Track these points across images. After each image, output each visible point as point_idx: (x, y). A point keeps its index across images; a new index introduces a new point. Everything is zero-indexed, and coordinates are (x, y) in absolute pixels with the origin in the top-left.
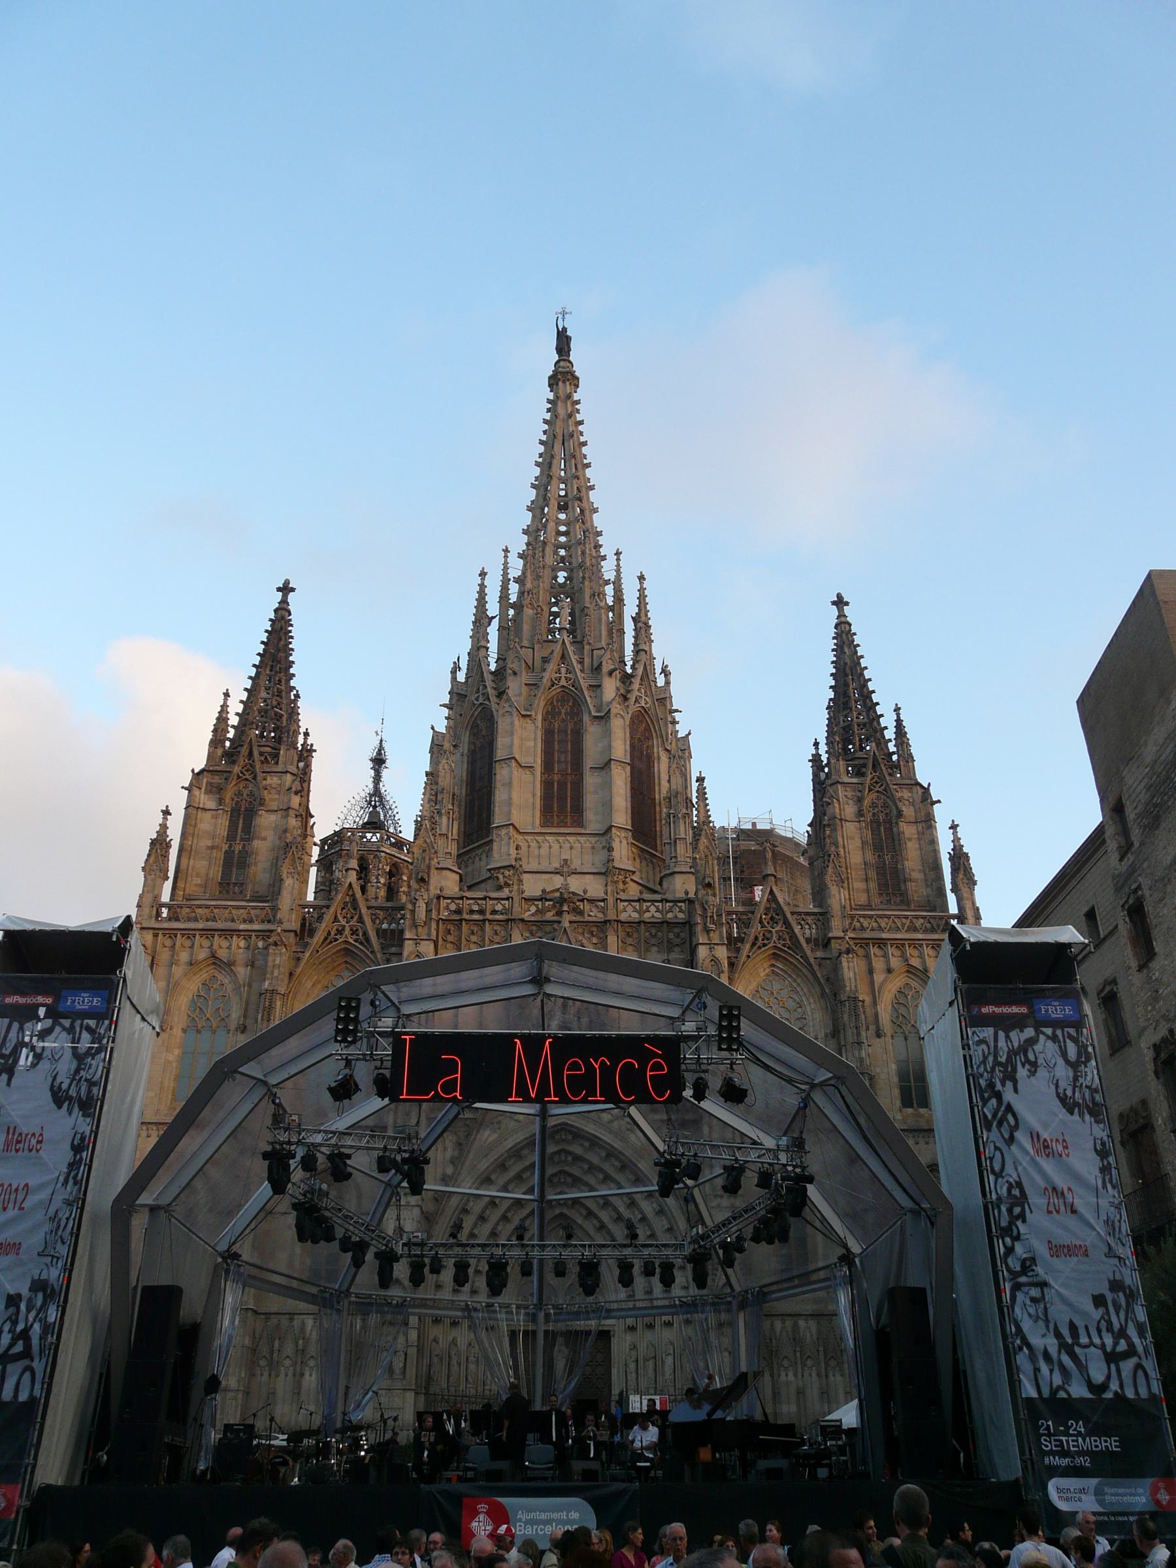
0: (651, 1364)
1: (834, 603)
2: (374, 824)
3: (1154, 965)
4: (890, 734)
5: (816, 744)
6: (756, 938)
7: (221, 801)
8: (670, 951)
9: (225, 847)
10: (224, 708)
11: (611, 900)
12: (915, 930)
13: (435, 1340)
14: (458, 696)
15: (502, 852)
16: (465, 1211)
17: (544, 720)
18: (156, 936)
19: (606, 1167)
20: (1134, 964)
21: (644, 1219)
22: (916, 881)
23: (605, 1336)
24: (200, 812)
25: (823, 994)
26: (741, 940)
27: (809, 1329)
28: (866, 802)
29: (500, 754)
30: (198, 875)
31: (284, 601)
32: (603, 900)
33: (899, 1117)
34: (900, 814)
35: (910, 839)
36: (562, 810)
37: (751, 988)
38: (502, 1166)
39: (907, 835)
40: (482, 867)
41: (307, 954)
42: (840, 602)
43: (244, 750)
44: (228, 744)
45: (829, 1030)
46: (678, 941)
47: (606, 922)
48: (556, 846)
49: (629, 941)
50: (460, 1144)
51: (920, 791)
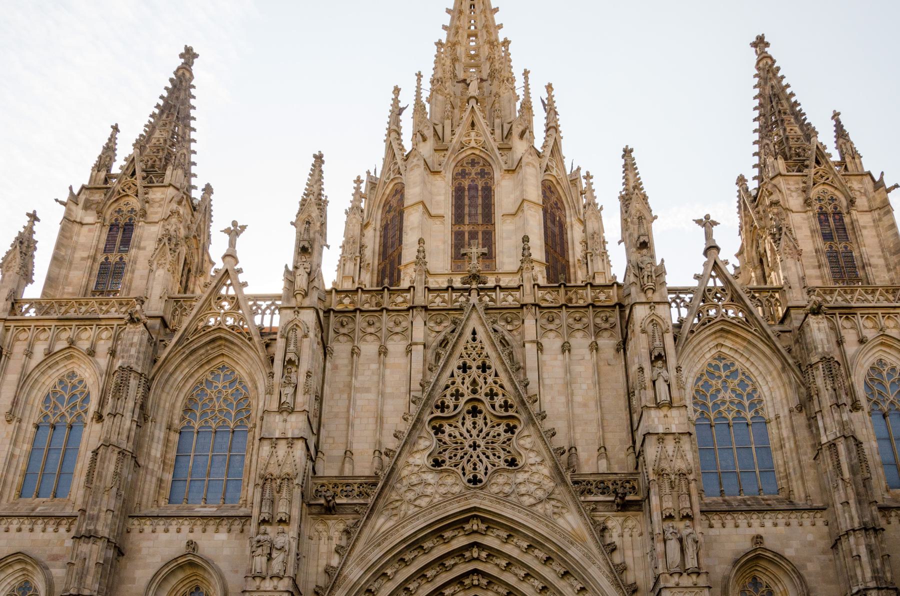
7: (99, 213)
9: (101, 258)
10: (112, 139)
11: (528, 286)
19: (528, 559)
22: (876, 266)
24: (76, 227)
28: (813, 193)
30: (69, 284)
32: (518, 288)
33: (886, 496)
34: (852, 202)
35: (865, 227)
37: (695, 370)
45: (793, 405)
47: (522, 306)
49: (551, 326)
50: (347, 532)
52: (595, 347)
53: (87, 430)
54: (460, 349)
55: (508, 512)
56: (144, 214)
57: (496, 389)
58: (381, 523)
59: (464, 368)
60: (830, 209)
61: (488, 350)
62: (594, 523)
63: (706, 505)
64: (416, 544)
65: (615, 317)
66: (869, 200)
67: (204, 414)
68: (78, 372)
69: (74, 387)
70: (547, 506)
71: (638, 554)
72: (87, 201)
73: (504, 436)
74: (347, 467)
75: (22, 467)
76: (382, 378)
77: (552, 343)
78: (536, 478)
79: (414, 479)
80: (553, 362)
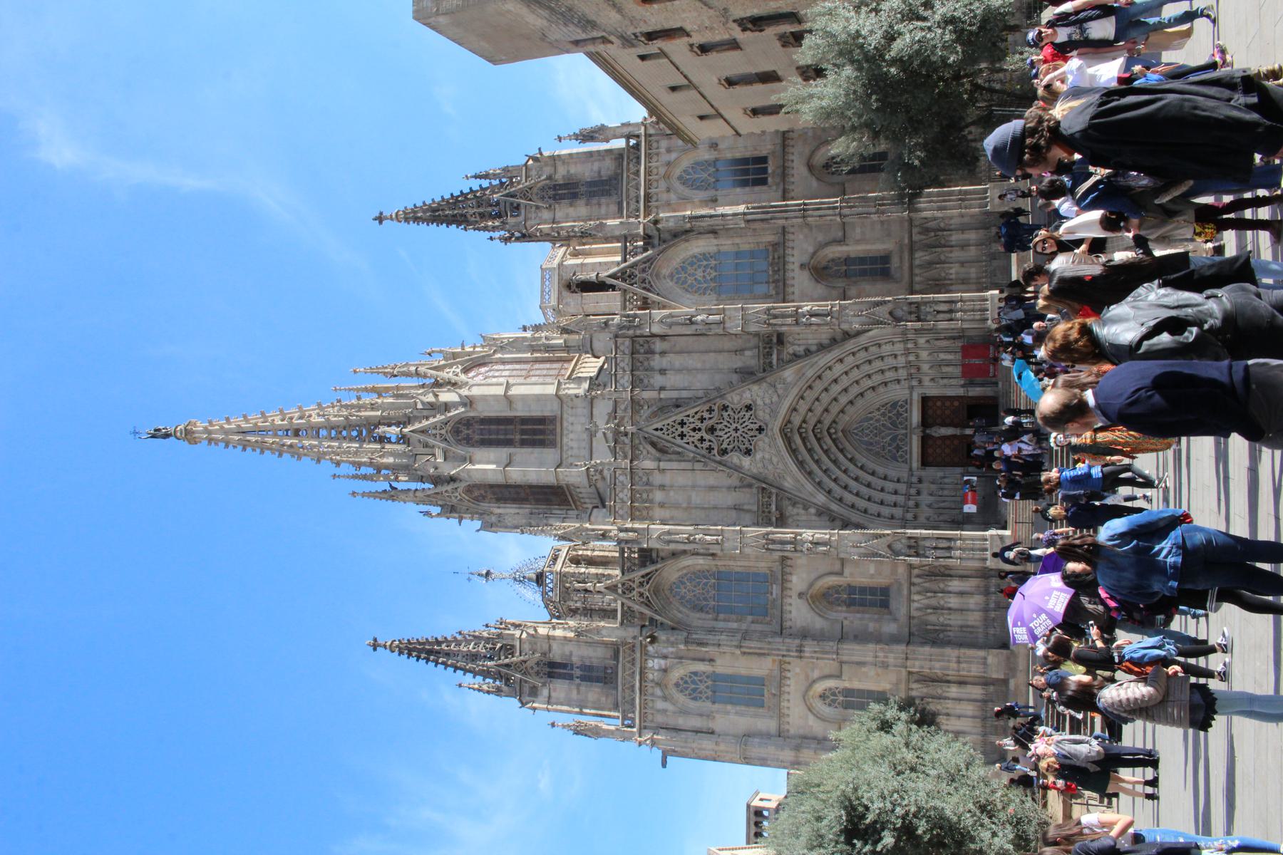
0: (945, 369)
1: (381, 222)
2: (540, 579)
3: (688, 28)
4: (485, 183)
5: (491, 238)
6: (644, 288)
7: (544, 685)
8: (653, 352)
9: (578, 681)
12: (638, 171)
13: (928, 519)
14: (450, 510)
15: (573, 475)
16: (841, 500)
17: (473, 446)
18: (645, 728)
20: (686, 39)
21: (846, 373)
23: (925, 400)
25: (687, 241)
26: (645, 300)
27: (921, 257)
29: (500, 479)
31: (385, 647)
34: (550, 178)
36: (542, 432)
38: (810, 473)
39: (565, 173)
40: (585, 491)
41: (658, 617)
42: (380, 219)
43: (504, 670)
44: (498, 683)
46: (646, 346)
48: (571, 436)
49: (646, 381)
50: (794, 504)
51: (531, 162)
52: (663, 353)
53: (719, 670)
54: (669, 438)
55: (783, 410)
56: (544, 654)
57: (697, 417)
58: (788, 483)
59: (682, 436)
60: (551, 193)
61: (670, 421)
62: (790, 361)
63: (777, 294)
64: (801, 464)
65: (641, 340)
66: (546, 165)
67: (705, 599)
68: (675, 681)
69: (686, 682)
70: (779, 386)
71: (810, 336)
72: (530, 695)
73: (730, 412)
74: (746, 507)
75: (743, 708)
76: (683, 488)
77: (658, 380)
78: (761, 394)
79: (760, 465)
80: (672, 380)
